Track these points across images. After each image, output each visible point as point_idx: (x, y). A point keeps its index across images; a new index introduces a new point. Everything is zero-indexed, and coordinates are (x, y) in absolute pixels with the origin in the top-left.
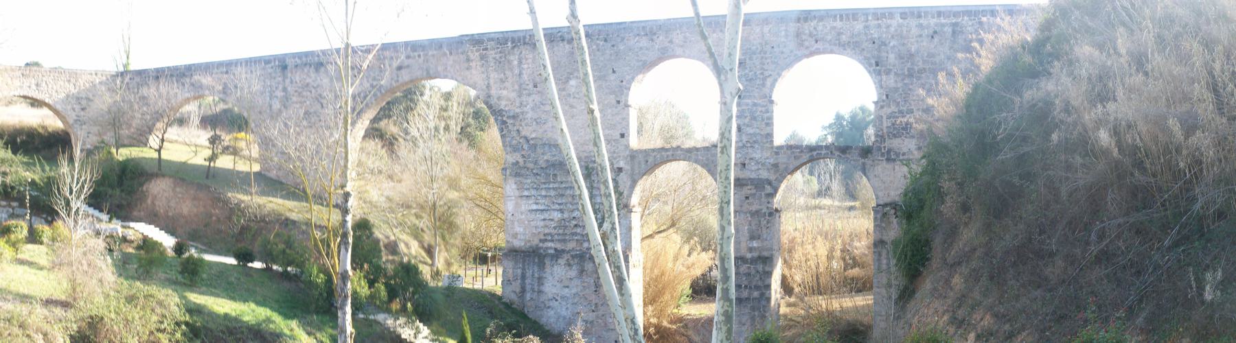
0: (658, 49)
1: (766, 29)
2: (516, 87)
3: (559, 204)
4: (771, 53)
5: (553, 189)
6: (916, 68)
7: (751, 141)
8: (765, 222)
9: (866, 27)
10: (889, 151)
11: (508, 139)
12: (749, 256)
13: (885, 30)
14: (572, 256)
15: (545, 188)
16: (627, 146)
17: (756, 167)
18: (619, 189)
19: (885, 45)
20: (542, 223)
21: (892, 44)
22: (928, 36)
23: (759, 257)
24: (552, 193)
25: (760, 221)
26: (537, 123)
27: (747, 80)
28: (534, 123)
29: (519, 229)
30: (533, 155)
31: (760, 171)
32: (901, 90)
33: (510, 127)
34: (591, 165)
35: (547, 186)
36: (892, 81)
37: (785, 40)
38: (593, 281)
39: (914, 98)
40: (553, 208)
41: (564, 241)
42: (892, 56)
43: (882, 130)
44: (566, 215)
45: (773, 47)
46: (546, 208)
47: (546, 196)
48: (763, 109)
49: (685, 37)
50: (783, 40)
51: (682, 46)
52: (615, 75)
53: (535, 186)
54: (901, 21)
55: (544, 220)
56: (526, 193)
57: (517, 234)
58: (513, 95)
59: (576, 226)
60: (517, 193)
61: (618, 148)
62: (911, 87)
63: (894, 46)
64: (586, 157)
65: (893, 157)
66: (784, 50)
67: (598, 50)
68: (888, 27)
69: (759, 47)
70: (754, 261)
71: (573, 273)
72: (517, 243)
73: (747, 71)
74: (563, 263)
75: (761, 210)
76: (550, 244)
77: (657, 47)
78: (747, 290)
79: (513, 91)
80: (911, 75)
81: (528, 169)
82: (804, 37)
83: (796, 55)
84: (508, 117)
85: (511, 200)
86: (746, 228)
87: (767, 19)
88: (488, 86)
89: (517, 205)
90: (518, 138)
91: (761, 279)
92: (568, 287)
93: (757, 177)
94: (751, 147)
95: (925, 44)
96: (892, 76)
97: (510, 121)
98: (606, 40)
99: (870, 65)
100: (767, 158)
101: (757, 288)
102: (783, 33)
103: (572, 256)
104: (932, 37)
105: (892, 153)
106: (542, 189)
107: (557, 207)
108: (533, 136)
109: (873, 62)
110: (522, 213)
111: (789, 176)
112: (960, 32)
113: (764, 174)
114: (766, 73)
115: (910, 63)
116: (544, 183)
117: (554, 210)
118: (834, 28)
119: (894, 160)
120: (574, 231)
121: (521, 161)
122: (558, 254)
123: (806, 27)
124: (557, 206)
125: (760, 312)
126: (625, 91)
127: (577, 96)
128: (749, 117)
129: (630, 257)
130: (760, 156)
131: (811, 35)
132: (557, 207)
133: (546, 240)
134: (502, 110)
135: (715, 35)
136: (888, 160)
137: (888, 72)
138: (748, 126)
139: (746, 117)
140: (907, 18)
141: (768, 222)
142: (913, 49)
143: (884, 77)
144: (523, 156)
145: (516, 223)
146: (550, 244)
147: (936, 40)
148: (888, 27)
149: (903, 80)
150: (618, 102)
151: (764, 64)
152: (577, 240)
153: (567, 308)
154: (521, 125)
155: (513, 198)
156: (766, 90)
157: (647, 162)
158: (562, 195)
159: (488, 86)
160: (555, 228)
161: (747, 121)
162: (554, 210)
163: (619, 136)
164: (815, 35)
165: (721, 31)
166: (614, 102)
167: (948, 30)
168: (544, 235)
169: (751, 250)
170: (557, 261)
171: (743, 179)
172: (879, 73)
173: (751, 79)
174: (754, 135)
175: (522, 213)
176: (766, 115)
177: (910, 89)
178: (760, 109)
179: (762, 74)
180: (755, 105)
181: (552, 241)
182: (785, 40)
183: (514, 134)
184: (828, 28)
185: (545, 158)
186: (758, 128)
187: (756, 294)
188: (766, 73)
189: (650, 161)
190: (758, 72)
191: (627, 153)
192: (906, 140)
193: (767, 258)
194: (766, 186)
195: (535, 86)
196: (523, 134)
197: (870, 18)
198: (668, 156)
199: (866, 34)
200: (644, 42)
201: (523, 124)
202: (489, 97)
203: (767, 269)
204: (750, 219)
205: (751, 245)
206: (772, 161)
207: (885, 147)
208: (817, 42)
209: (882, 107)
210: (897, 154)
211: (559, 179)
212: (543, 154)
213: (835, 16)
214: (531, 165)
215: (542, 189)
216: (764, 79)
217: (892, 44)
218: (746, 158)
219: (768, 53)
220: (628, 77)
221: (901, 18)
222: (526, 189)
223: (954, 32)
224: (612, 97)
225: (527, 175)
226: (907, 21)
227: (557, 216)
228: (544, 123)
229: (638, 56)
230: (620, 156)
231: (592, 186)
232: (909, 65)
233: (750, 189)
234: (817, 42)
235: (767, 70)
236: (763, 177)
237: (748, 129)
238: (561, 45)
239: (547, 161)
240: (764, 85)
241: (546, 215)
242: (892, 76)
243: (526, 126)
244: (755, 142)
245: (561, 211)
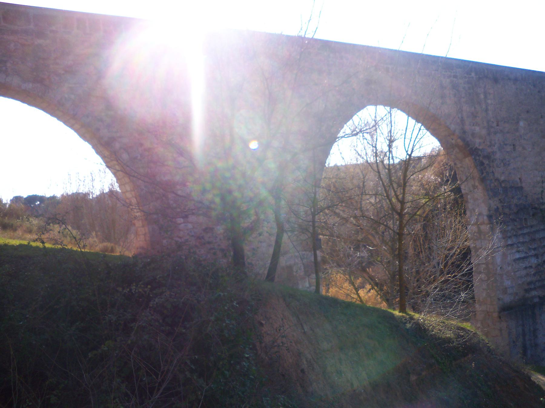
3: (535, 249)
15: (522, 234)
20: (524, 272)
24: (527, 239)
29: (507, 283)
40: (530, 254)
55: (526, 268)
57: (506, 288)
58: (484, 132)
72: (508, 299)
76: (534, 293)
88: (462, 120)
89: (504, 255)
97: (486, 162)
106: (520, 235)
107: (533, 252)
108: (503, 178)
110: (509, 264)
124: (533, 252)
132: (533, 252)
133: (531, 289)
134: (476, 149)
145: (505, 276)
146: (534, 293)
159: (462, 120)
160: (534, 275)
162: (532, 256)
168: (529, 283)
175: (509, 264)
181: (535, 289)
202: (464, 132)
215: (520, 235)
227: (534, 261)
241: (526, 264)
245: (536, 256)
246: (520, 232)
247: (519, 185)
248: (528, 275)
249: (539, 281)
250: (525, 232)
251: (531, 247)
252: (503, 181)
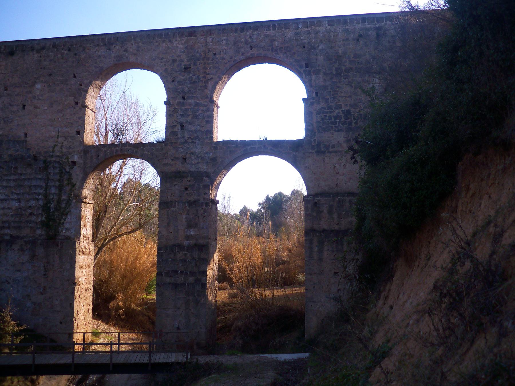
0: (114, 57)
1: (209, 39)
3: (18, 194)
4: (213, 59)
5: (14, 180)
6: (343, 68)
7: (192, 138)
8: (202, 211)
9: (297, 34)
10: (319, 145)
12: (186, 243)
13: (314, 36)
14: (25, 241)
15: (6, 180)
16: (82, 142)
17: (196, 161)
18: (72, 181)
19: (314, 48)
21: (320, 48)
22: (354, 39)
23: (196, 245)
24: (12, 184)
25: (197, 211)
26: (5, 121)
27: (191, 83)
31: (199, 164)
32: (329, 88)
34: (49, 159)
35: (8, 178)
36: (321, 80)
37: (226, 48)
38: (42, 265)
39: (342, 95)
40: (12, 197)
41: (19, 228)
42: (321, 58)
43: (312, 125)
44: (22, 204)
45: (215, 54)
46: (6, 198)
47: (6, 187)
48: (204, 108)
49: (138, 47)
50: (224, 47)
51: (135, 54)
52: (75, 79)
54: (328, 27)
55: (3, 208)
59: (31, 214)
61: (73, 143)
62: (339, 85)
63: (323, 49)
64: (45, 152)
65: (323, 149)
66: (225, 56)
67: (62, 58)
68: (317, 33)
69: (202, 54)
70: (190, 248)
71: (25, 258)
73: (191, 75)
74: (16, 249)
75: (199, 200)
76: (6, 231)
77: (113, 55)
78: (183, 276)
80: (338, 74)
82: (240, 45)
83: (235, 60)
86: (184, 217)
87: (210, 31)
91: (196, 265)
92: (19, 271)
93: (197, 170)
94: (193, 142)
95: (351, 46)
96: (321, 75)
98: (69, 50)
99: (301, 67)
100: (207, 153)
101: (192, 273)
102: (224, 42)
103: (25, 241)
104: (358, 40)
105: (322, 146)
106: (4, 180)
107: (15, 196)
109: (303, 64)
111: (225, 171)
112: (383, 34)
113: (203, 168)
114: (208, 77)
115: (337, 64)
116: (6, 175)
117: (12, 199)
118: (267, 36)
119: (324, 152)
120: (29, 219)
122: (13, 239)
123: (243, 36)
124: (15, 196)
125: (195, 296)
126: (83, 93)
127: (41, 98)
128: (191, 116)
129: (77, 245)
130: (200, 151)
131: (246, 43)
132: (15, 196)
135: (164, 45)
136: (319, 152)
137: (317, 72)
138: (190, 123)
139: (188, 115)
140: (333, 25)
141: (205, 212)
142: (340, 51)
143: (314, 77)
146: (6, 231)
147: (361, 42)
148: (317, 33)
149: (332, 78)
150: (77, 103)
151: (206, 69)
152: (31, 227)
153: (18, 291)
156: (208, 92)
157: (98, 156)
158: (21, 186)
160: (12, 216)
161: (189, 119)
162: (12, 199)
163: (75, 133)
164: (250, 43)
165: (170, 41)
166: (73, 103)
167: (372, 33)
169: (188, 237)
170: (11, 246)
171: (183, 172)
172: (309, 74)
173: (194, 82)
174: (196, 131)
176: (206, 114)
177: (338, 87)
178: (202, 108)
179: (205, 77)
180: (197, 104)
181: (9, 228)
182: (226, 48)
184: (263, 36)
185: (9, 152)
186: (199, 125)
187: (191, 279)
188: (208, 77)
189: (101, 155)
190: (201, 76)
191: (82, 148)
192: (335, 133)
193: (203, 246)
194: (204, 178)
197: (300, 26)
198: (117, 151)
199: (296, 40)
200: (103, 51)
203: (203, 256)
204: (188, 208)
205: (188, 234)
206: (210, 155)
207: (315, 141)
208: (251, 49)
209: (312, 104)
210: (327, 147)
211: (19, 172)
212: (7, 149)
213: (269, 26)
215: (4, 180)
216: (207, 82)
217: (320, 48)
218: (187, 153)
219: (211, 59)
220: (86, 81)
221: (329, 25)
223: (378, 36)
224: (72, 98)
226: (334, 27)
227: (15, 204)
228: (11, 122)
229: (96, 63)
230: (74, 151)
231: (48, 178)
232: (336, 65)
233: (190, 181)
234: (251, 48)
235: (209, 74)
236: (202, 170)
237: (190, 126)
238: (31, 54)
240: (206, 87)
241: (6, 205)
242: (321, 75)
244: (196, 138)
245: (19, 200)
246: (5, 178)
247: (23, 139)
248: (5, 214)
249: (15, 222)
250: (12, 178)
251: (14, 191)
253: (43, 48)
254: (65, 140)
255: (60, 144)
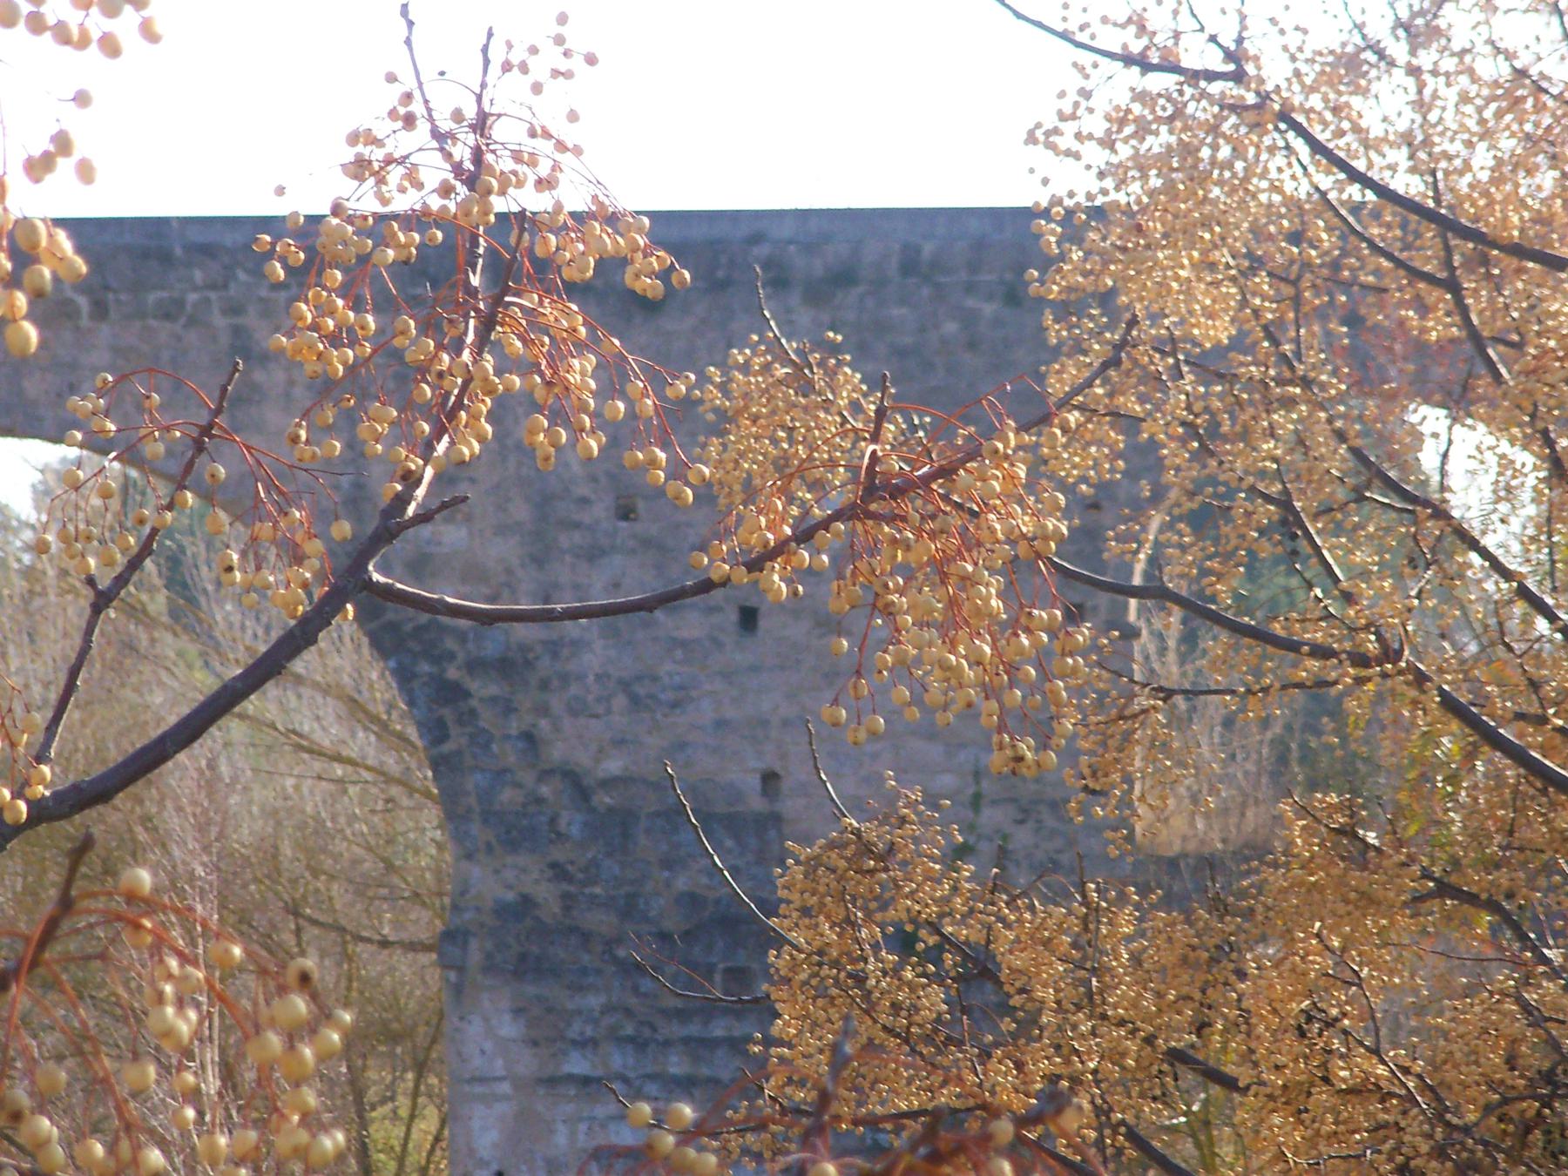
2: (521, 511)
11: (474, 782)
15: (687, 1041)
26: (635, 701)
28: (620, 701)
30: (611, 867)
33: (487, 718)
35: (694, 1029)
53: (629, 1030)
56: (577, 1064)
58: (502, 551)
60: (527, 1063)
67: (972, 345)
79: (502, 530)
81: (586, 937)
84: (475, 666)
85: (489, 1100)
90: (528, 777)
97: (483, 688)
106: (667, 1044)
108: (614, 766)
116: (682, 1015)
121: (546, 894)
144: (559, 872)
154: (543, 710)
155: (505, 1088)
183: (509, 755)
185: (682, 883)
195: (626, 513)
196: (556, 753)
201: (556, 703)
212: (668, 864)
214: (600, 921)
215: (667, 1044)
222: (583, 1044)
225: (584, 971)
228: (675, 705)
239: (693, 900)
243: (574, 713)
247: (757, 803)
252: (609, 783)
253: (843, 277)
254: (1021, 822)
255: (991, 840)
